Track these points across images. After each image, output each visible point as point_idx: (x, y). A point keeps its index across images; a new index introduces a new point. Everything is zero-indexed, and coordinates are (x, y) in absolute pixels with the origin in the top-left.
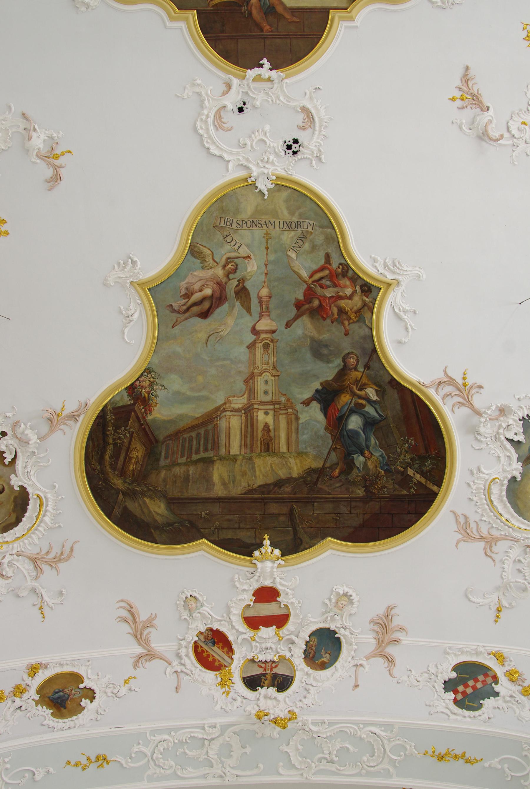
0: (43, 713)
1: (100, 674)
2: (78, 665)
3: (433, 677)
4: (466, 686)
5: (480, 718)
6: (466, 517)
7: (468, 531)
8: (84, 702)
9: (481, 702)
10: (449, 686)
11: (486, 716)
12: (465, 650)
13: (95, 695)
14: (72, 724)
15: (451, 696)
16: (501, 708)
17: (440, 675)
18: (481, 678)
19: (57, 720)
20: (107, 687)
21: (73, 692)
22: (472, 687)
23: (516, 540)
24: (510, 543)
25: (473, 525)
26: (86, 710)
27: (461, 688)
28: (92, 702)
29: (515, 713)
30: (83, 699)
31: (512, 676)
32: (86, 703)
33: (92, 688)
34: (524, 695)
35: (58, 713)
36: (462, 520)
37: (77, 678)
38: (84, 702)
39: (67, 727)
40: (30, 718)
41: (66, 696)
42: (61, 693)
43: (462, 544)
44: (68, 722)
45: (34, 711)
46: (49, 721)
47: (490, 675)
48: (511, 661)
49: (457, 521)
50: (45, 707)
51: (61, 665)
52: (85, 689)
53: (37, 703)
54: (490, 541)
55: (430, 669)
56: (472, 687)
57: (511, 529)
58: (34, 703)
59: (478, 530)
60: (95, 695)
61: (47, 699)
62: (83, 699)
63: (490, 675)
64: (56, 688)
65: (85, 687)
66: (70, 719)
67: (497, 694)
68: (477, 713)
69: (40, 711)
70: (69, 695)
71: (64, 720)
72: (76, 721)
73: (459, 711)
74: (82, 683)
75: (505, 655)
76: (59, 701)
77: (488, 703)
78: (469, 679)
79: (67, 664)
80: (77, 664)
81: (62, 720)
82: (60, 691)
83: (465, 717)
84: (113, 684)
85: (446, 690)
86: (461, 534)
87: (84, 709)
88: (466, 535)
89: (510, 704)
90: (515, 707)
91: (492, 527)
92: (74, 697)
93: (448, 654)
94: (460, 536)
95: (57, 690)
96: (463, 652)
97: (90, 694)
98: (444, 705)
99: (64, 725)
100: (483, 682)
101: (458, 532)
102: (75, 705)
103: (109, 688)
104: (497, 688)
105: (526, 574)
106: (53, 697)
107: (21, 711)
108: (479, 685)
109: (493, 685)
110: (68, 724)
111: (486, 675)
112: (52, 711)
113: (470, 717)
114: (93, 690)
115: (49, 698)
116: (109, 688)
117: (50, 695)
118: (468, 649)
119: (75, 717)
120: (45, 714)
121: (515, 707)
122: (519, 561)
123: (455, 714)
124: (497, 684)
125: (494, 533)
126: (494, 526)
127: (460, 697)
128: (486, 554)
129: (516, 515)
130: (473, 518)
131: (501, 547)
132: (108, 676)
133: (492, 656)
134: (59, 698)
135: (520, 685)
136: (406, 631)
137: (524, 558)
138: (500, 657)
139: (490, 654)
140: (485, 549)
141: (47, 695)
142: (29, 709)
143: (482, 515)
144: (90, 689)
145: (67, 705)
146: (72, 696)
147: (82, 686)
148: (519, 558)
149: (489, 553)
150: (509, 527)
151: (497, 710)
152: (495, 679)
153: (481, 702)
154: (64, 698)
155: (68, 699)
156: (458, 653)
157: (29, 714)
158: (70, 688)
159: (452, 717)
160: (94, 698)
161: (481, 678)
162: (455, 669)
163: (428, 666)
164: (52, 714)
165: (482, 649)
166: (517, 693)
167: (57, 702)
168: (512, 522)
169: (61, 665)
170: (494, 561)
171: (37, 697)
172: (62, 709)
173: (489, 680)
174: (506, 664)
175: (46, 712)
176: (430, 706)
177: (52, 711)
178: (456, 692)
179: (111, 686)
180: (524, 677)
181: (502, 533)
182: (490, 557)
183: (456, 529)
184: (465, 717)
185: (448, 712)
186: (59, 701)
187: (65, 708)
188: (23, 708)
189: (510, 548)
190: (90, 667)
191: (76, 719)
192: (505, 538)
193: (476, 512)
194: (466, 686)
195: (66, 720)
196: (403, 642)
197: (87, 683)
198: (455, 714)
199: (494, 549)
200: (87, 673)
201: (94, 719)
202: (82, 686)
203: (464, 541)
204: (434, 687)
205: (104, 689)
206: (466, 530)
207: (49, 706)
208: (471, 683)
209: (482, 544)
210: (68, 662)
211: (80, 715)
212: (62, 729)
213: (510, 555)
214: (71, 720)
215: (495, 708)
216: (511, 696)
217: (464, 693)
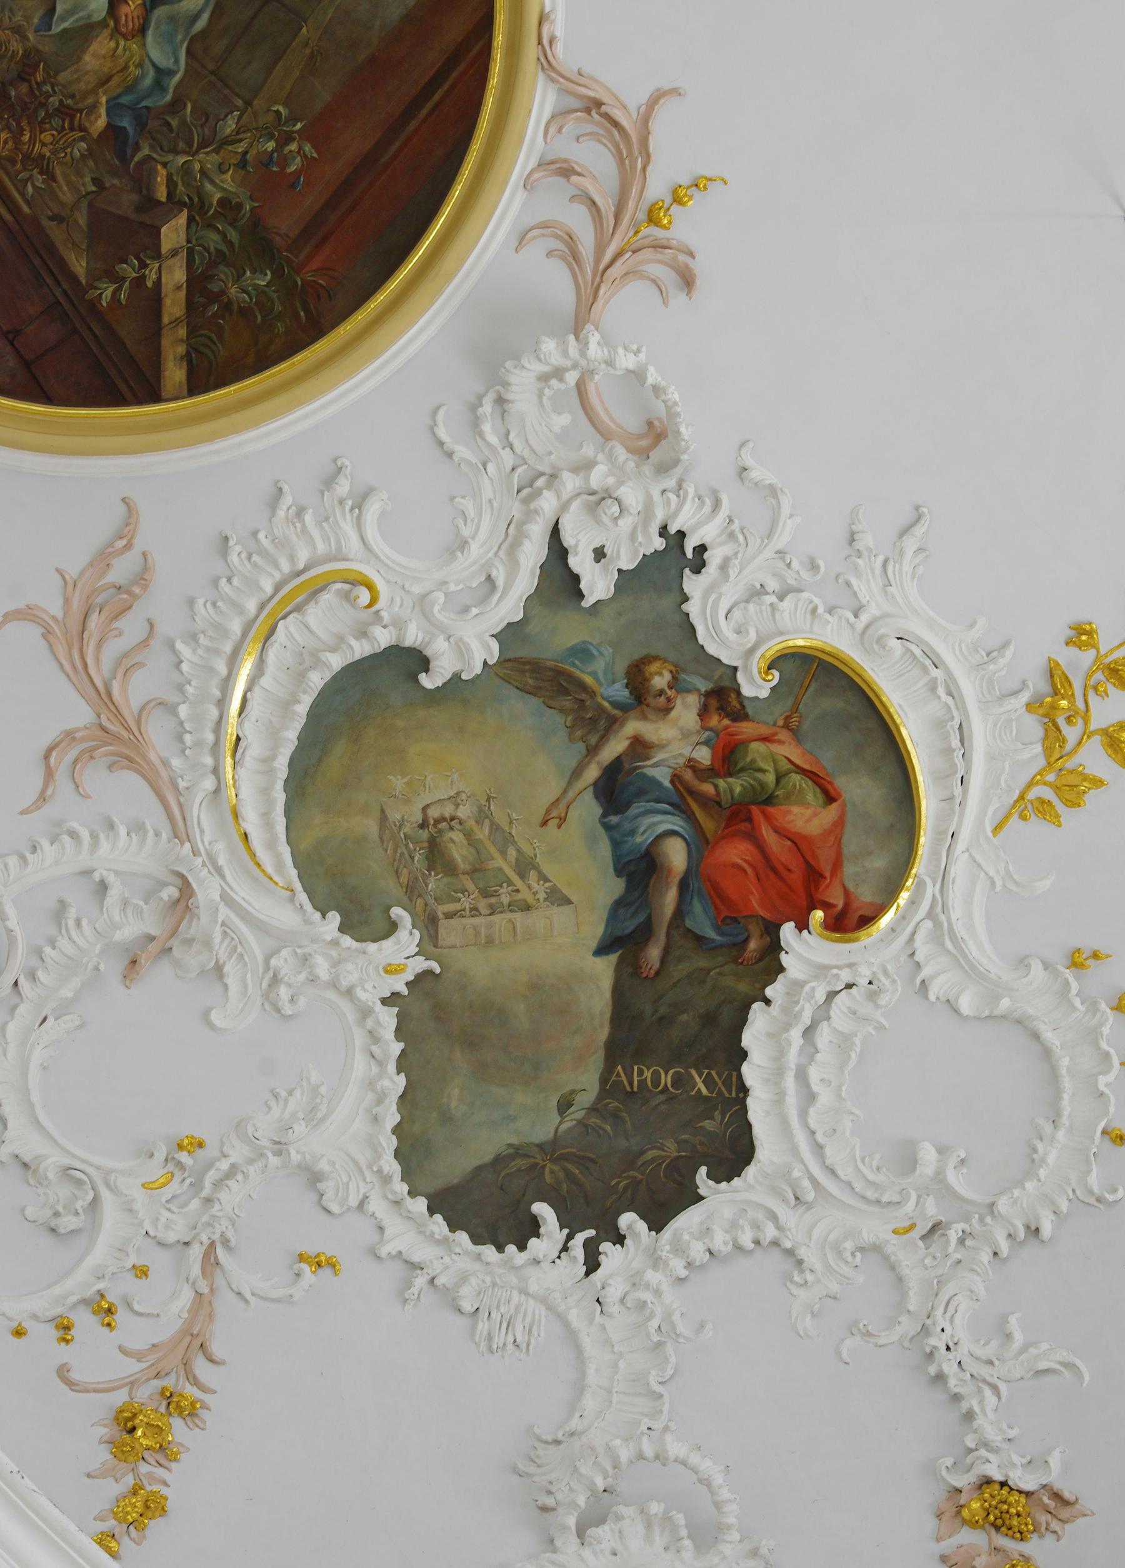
6: (143, 577)
7: (94, 621)
23: (180, 831)
24: (153, 816)
25: (131, 628)
36: (121, 571)
43: (31, 633)
49: (103, 558)
54: (115, 738)
57: (209, 784)
59: (127, 664)
86: (67, 601)
88: (74, 626)
91: (173, 710)
94: (55, 607)
101: (69, 586)
105: (63, 943)
122: (103, 887)
125: (157, 735)
126: (183, 711)
128: (47, 756)
129: (283, 772)
130: (161, 606)
131: (120, 792)
137: (125, 903)
140: (69, 736)
143: (192, 638)
148: (111, 878)
149: (63, 762)
150: (216, 771)
168: (241, 772)
170: (43, 798)
181: (176, 763)
182: (49, 774)
183: (72, 572)
189: (137, 828)
192: (165, 791)
193: (191, 602)
199: (95, 777)
203: (47, 634)
206: (93, 614)
209: (80, 714)
213: (105, 846)
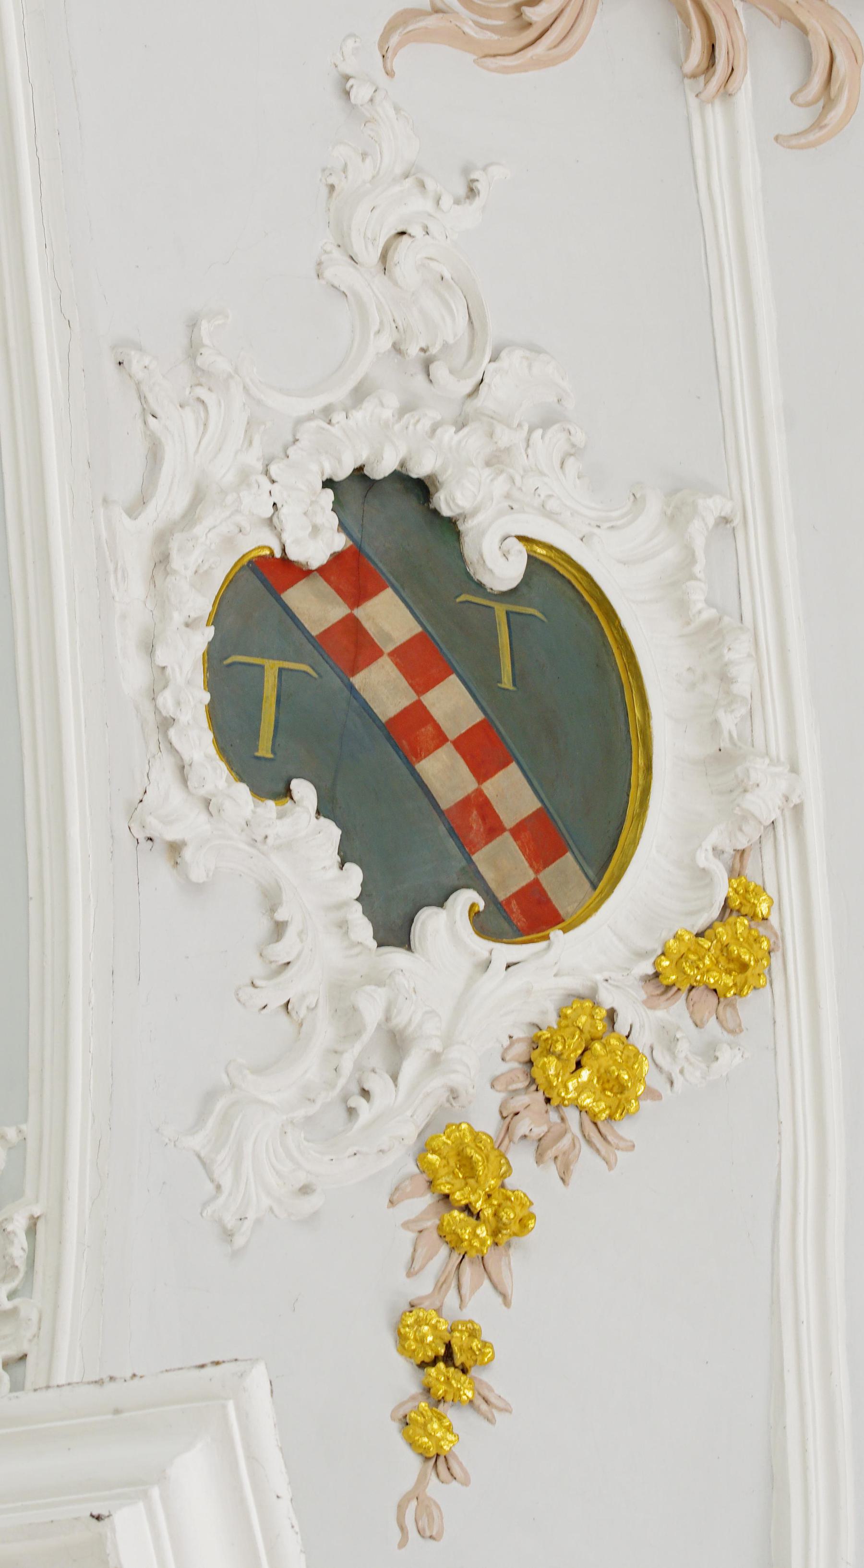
3: (452, 384)
4: (421, 663)
5: (164, 773)
9: (304, 791)
10: (397, 518)
11: (187, 823)
12: (738, 651)
15: (316, 537)
16: (282, 951)
17: (473, 442)
18: (512, 794)
22: (416, 718)
27: (389, 618)
29: (259, 1070)
31: (573, 1067)
34: (425, 1148)
47: (549, 878)
48: (710, 1054)
55: (512, 360)
56: (416, 718)
63: (549, 878)
67: (395, 932)
68: (198, 742)
73: (196, 602)
75: (751, 1008)
77: (300, 846)
78: (481, 686)
83: (149, 649)
85: (354, 490)
89: (324, 1031)
90: (310, 1067)
93: (676, 517)
96: (710, 636)
98: (224, 471)
100: (479, 804)
104: (445, 928)
108: (445, 774)
109: (467, 898)
111: (542, 839)
113: (160, 678)
118: (744, 679)
121: (310, 1067)
123: (162, 561)
124: (482, 924)
127: (316, 607)
133: (722, 889)
135: (509, 1117)
136: (818, 124)
138: (721, 961)
139: (734, 873)
151: (262, 926)
152: (528, 916)
153: (304, 791)
156: (698, 595)
159: (134, 538)
161: (512, 794)
162: (552, 575)
163: (535, 349)
165: (764, 802)
166: (437, 1084)
173: (505, 865)
174: (675, 1011)
176: (193, 350)
178: (351, 574)
180: (587, 1160)
184: (149, 649)
185: (170, 500)
194: (421, 663)
196: (716, 114)
198: (162, 561)
204: (360, 394)
208: (452, 704)
215: (271, 899)
216: (396, 1042)
217: (352, 645)
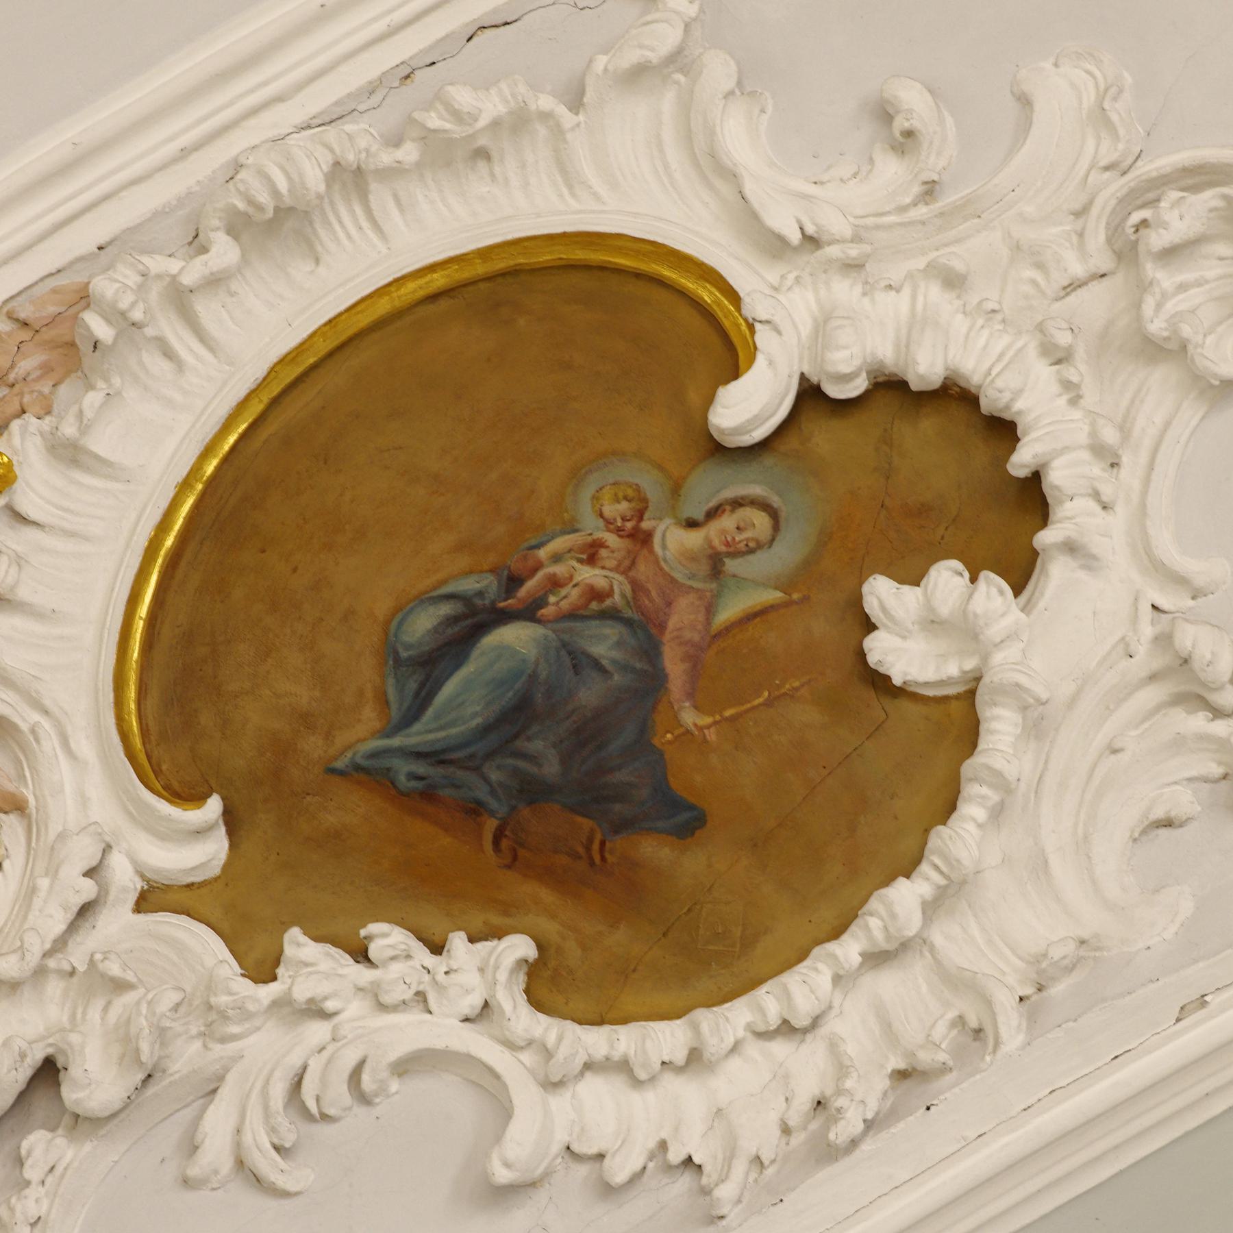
0: (410, 1032)
1: (914, 101)
2: (518, 122)
8: (917, 626)
13: (1021, 461)
14: (910, 1003)
19: (667, 1039)
20: (1126, 252)
21: (674, 542)
26: (1001, 729)
28: (1020, 572)
30: (880, 592)
32: (962, 630)
33: (926, 370)
35: (619, 939)
37: (603, 322)
38: (917, 626)
39: (867, 1092)
40: (267, 1164)
41: (604, 643)
42: (515, 637)
44: (839, 1005)
45: (266, 1051)
46: (560, 1103)
50: (387, 938)
51: (277, 226)
52: (823, 436)
53: (246, 919)
58: (206, 947)
60: (1021, 461)
61: (352, 809)
62: (880, 592)
64: (393, 583)
65: (810, 395)
66: (849, 949)
69: (354, 1010)
70: (644, 631)
71: (767, 1002)
72: (955, 941)
74: (730, 356)
76: (544, 753)
79: (351, 178)
80: (491, 106)
81: (738, 1016)
82: (474, 621)
84: (1197, 177)
87: (955, 719)
92: (727, 613)
95: (423, 625)
97: (945, 471)
99: (806, 1068)
102: (805, 714)
103: (1170, 254)
106: (418, 736)
107: (80, 1124)
110: (852, 1026)
112: (520, 947)
114: (955, 396)
115: (369, 774)
116: (1170, 254)
117: (361, 734)
119: (904, 898)
120: (442, 1030)
132: (1062, 90)
134: (520, 711)
141: (313, 746)
142: (188, 1056)
144: (890, 388)
145: (688, 776)
146: (683, 618)
147: (747, 406)
154: (590, 694)
155: (651, 682)
157: (217, 1123)
158: (596, 509)
160: (1032, 498)
164: (545, 985)
167: (532, 791)
169: (277, 226)
171: (193, 843)
172: (654, 850)
175: (445, 993)
177: (520, 947)
179: (1180, 217)
186: (544, 753)
187: (686, 820)
188: (95, 1082)
190: (718, 71)
191: (931, 908)
195: (805, 986)
197: (805, 330)
200: (717, 170)
201: (1184, 801)
202: (747, 406)
205: (1095, 304)
207: (442, 901)
210: (360, 140)
211: (963, 837)
212: (819, 1136)
214: (876, 959)
